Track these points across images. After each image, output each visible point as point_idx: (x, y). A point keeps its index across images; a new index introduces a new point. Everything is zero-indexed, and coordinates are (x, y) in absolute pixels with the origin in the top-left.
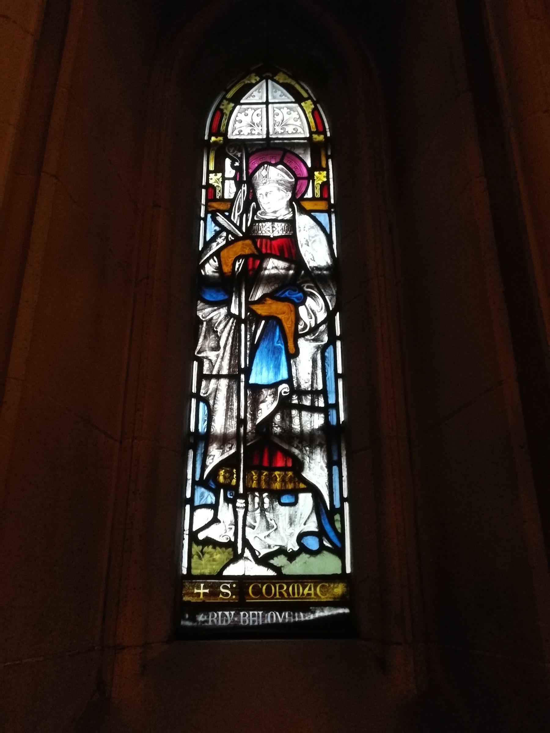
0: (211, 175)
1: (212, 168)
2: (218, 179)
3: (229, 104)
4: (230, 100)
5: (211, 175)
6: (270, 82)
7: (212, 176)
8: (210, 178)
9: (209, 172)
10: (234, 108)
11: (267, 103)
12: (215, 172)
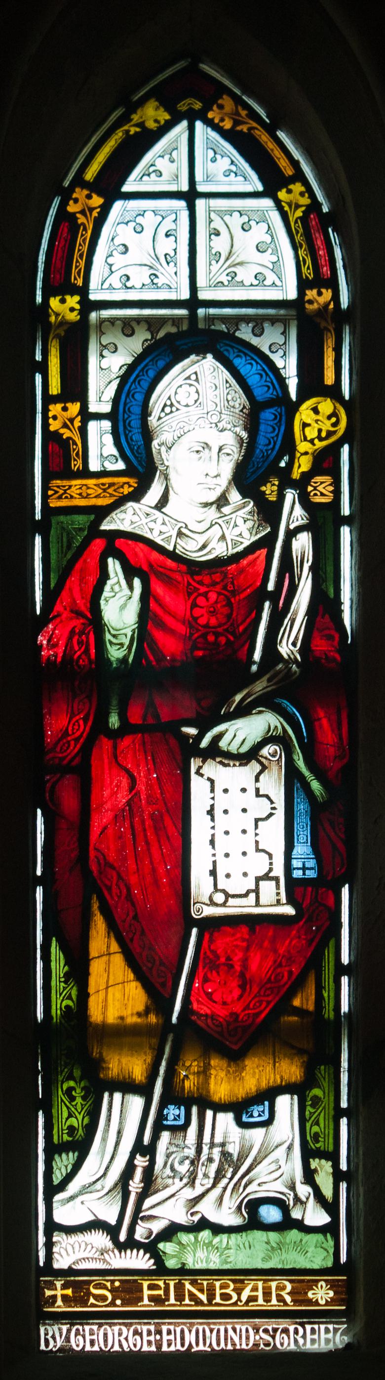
0: (51, 407)
1: (55, 388)
2: (72, 420)
3: (89, 197)
4: (94, 187)
5: (51, 407)
6: (199, 125)
7: (55, 409)
8: (51, 414)
9: (48, 399)
10: (105, 210)
11: (191, 196)
12: (65, 397)
